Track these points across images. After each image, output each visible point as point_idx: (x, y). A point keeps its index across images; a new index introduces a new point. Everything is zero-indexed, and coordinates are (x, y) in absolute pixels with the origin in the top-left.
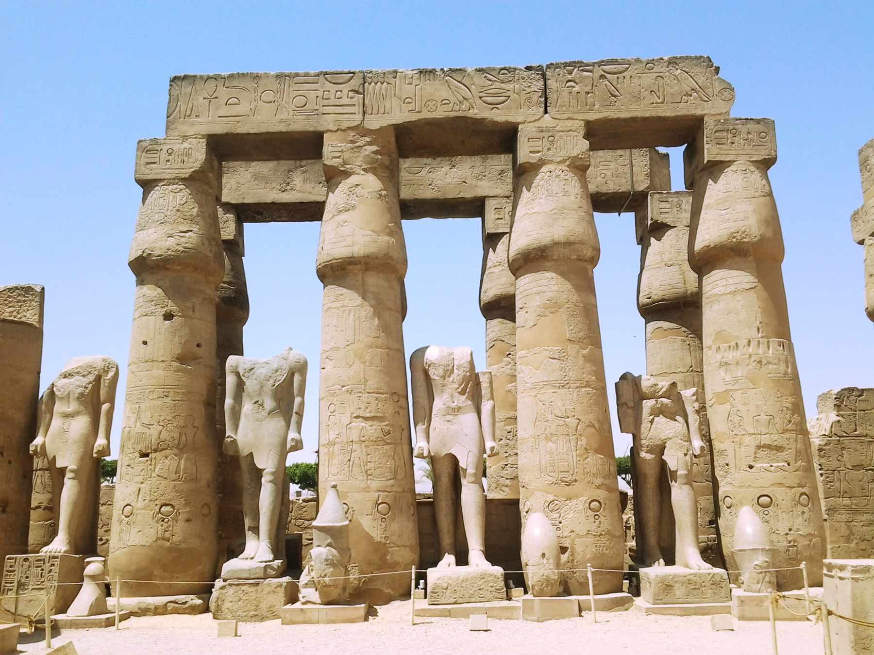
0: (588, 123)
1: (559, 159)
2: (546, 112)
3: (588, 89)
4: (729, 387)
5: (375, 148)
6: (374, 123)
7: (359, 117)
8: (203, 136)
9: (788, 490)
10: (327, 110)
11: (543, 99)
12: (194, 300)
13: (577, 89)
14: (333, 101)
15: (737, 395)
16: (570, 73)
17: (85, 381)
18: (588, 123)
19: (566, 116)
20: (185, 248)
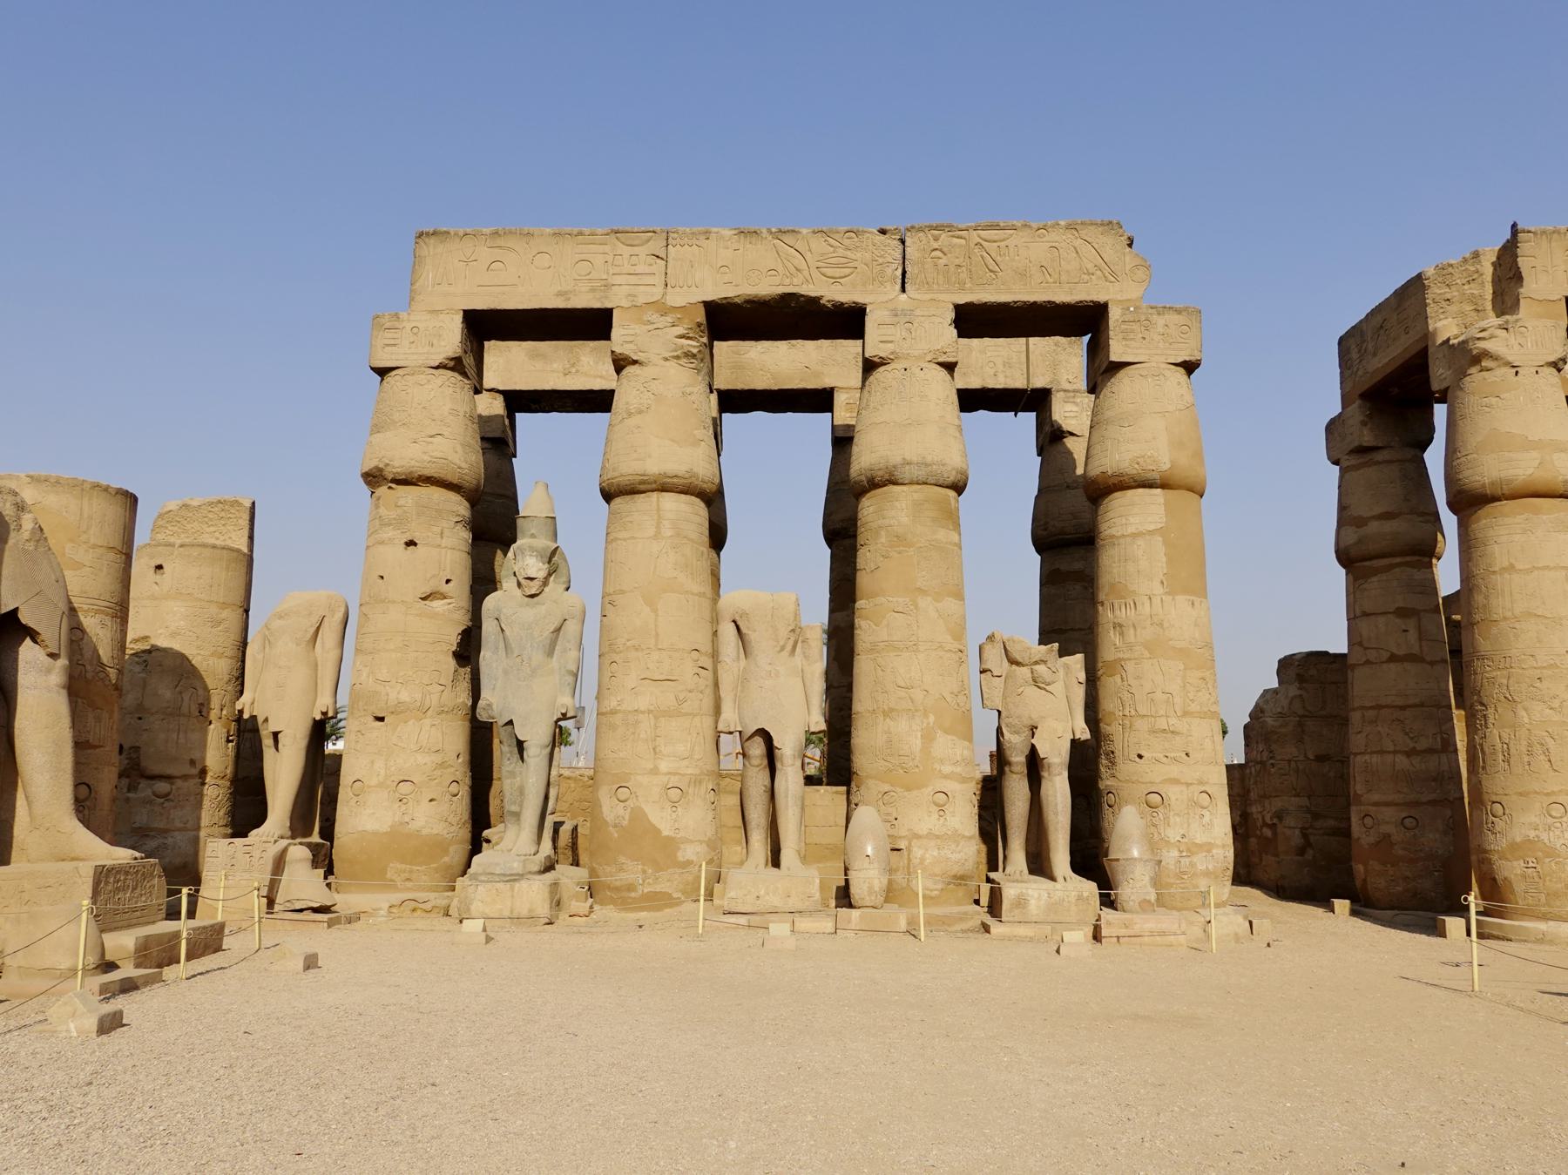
0: (957, 307)
1: (916, 353)
2: (903, 290)
3: (957, 262)
4: (1121, 655)
5: (680, 330)
6: (677, 299)
7: (659, 290)
9: (1184, 788)
10: (618, 280)
11: (899, 272)
13: (942, 262)
14: (627, 268)
15: (1130, 666)
16: (936, 239)
18: (957, 307)
19: (928, 297)
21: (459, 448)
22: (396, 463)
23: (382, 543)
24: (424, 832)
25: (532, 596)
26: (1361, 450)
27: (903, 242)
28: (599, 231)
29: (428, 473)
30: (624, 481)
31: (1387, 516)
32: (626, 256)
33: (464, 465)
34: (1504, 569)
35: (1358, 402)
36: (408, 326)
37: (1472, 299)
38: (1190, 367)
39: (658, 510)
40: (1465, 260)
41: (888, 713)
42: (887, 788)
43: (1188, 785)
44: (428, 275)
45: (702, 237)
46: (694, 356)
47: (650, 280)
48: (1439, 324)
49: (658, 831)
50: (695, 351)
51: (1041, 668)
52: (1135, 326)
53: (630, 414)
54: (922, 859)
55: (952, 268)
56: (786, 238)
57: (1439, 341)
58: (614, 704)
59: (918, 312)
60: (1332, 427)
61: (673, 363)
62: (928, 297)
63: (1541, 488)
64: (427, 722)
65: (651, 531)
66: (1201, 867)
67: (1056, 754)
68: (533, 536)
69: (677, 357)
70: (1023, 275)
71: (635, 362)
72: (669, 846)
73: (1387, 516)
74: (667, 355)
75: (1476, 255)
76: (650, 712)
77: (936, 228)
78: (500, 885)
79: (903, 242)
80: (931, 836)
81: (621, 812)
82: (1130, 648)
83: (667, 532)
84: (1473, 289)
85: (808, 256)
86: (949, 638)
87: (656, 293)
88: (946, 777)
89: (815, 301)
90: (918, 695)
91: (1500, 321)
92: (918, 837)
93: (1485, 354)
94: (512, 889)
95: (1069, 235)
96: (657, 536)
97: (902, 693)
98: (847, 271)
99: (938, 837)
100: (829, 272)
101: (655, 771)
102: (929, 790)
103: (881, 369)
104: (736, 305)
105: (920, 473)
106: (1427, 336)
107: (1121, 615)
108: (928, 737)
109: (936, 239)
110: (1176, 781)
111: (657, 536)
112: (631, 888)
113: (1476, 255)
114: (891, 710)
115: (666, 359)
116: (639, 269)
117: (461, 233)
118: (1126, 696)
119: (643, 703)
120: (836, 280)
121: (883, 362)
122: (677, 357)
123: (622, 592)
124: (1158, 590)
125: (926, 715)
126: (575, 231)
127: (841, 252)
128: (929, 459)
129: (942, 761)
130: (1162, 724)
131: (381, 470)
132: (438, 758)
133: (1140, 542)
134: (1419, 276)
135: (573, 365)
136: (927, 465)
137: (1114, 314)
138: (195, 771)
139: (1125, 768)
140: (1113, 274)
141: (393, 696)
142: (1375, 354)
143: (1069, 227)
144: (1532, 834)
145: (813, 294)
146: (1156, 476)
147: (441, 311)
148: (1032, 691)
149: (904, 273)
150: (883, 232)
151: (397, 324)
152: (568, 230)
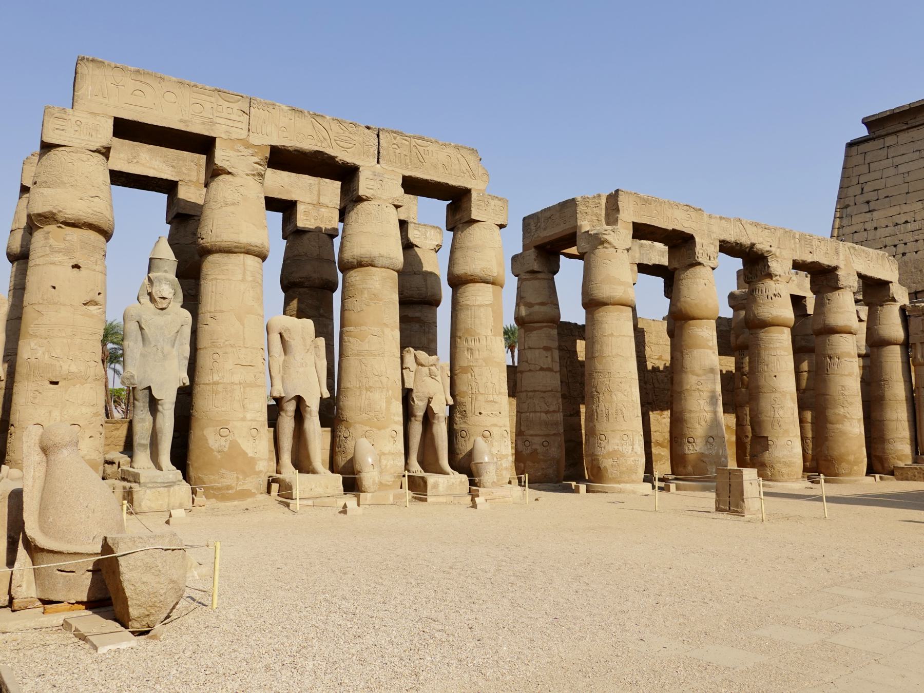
0: (404, 178)
2: (378, 162)
5: (256, 159)
6: (256, 140)
7: (245, 132)
13: (398, 151)
14: (225, 115)
15: (476, 370)
16: (395, 138)
18: (404, 178)
19: (390, 168)
22: (68, 211)
23: (54, 264)
25: (162, 309)
26: (533, 272)
27: (378, 136)
28: (208, 87)
29: (92, 220)
30: (224, 245)
31: (542, 304)
32: (225, 107)
34: (609, 335)
35: (533, 249)
36: (74, 119)
37: (597, 215)
38: (501, 226)
40: (594, 197)
41: (369, 389)
42: (368, 428)
44: (86, 88)
45: (271, 107)
47: (239, 125)
48: (583, 223)
49: (245, 454)
51: (433, 368)
52: (482, 203)
53: (227, 205)
54: (386, 465)
56: (318, 119)
57: (583, 231)
58: (216, 378)
59: (386, 176)
60: (515, 259)
61: (251, 178)
62: (390, 168)
63: (624, 302)
64: (88, 386)
65: (240, 277)
67: (441, 411)
68: (166, 271)
69: (254, 175)
70: (435, 167)
71: (229, 173)
72: (252, 462)
73: (542, 304)
74: (249, 172)
75: (599, 196)
76: (240, 384)
77: (395, 133)
78: (161, 490)
79: (378, 136)
80: (390, 453)
81: (223, 443)
82: (477, 360)
83: (249, 278)
84: (596, 210)
85: (330, 132)
87: (243, 134)
89: (333, 158)
90: (384, 380)
91: (609, 228)
92: (384, 454)
93: (606, 241)
94: (169, 491)
95: (455, 151)
96: (243, 280)
97: (376, 379)
100: (341, 144)
101: (244, 419)
102: (388, 430)
103: (366, 203)
104: (289, 151)
105: (386, 262)
106: (576, 227)
107: (472, 344)
109: (395, 138)
110: (495, 425)
111: (243, 280)
112: (228, 487)
113: (599, 196)
114: (371, 387)
115: (248, 175)
116: (232, 117)
117: (113, 65)
118: (473, 384)
119: (236, 378)
120: (345, 149)
121: (367, 199)
122: (254, 175)
123: (222, 311)
124: (489, 333)
125: (388, 391)
126: (192, 83)
127: (347, 134)
128: (392, 256)
130: (490, 398)
131: (54, 214)
133: (482, 309)
134: (574, 200)
135: (135, 157)
136: (391, 259)
137: (474, 195)
139: (472, 419)
140: (474, 175)
141: (65, 367)
142: (545, 229)
143: (457, 147)
144: (616, 448)
145: (333, 154)
146: (491, 278)
147: (98, 114)
148: (429, 379)
149: (379, 153)
150: (368, 128)
151: (65, 116)
152: (188, 81)
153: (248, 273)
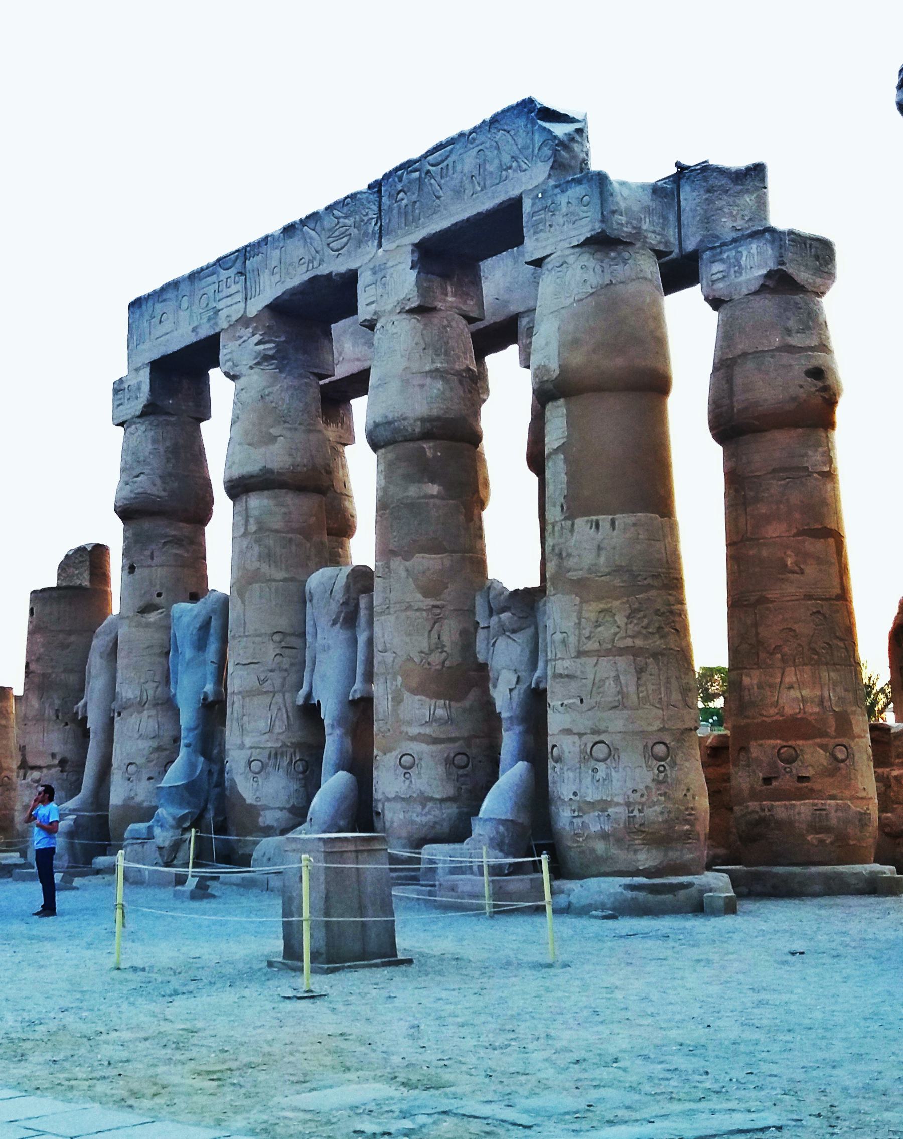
5: (257, 338)
8: (147, 364)
12: (153, 547)
17: (108, 638)
19: (394, 245)
20: (138, 494)
21: (158, 482)
24: (146, 804)
33: (163, 494)
39: (247, 509)
43: (580, 735)
46: (272, 357)
50: (271, 353)
54: (392, 822)
55: (410, 207)
66: (595, 828)
69: (258, 364)
80: (397, 798)
83: (253, 528)
86: (419, 596)
88: (413, 738)
92: (388, 800)
98: (345, 240)
99: (403, 799)
100: (334, 245)
101: (242, 746)
108: (398, 700)
115: (251, 368)
128: (390, 417)
129: (410, 723)
132: (155, 744)
138: (56, 762)
145: (327, 272)
153: (252, 520)
